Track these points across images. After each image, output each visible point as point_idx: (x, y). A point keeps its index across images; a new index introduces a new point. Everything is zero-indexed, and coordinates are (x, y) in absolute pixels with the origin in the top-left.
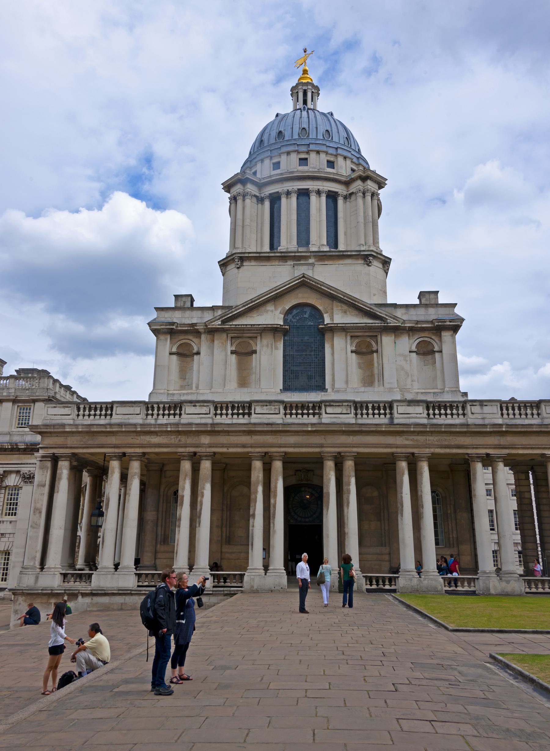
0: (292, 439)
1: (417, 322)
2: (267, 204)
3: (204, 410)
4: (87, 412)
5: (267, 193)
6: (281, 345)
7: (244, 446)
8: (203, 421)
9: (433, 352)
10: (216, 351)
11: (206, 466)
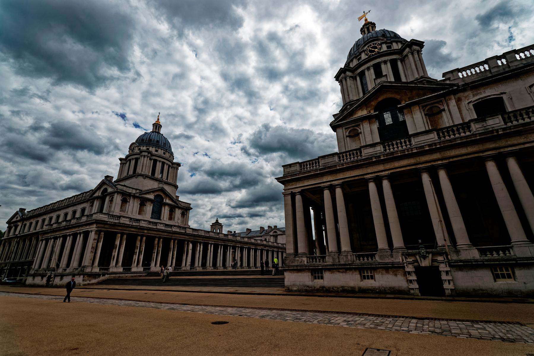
0: (166, 234)
1: (184, 207)
2: (152, 161)
3: (146, 223)
4: (111, 218)
5: (154, 158)
6: (152, 205)
7: (155, 234)
8: (144, 226)
9: (185, 214)
10: (135, 202)
11: (144, 238)
